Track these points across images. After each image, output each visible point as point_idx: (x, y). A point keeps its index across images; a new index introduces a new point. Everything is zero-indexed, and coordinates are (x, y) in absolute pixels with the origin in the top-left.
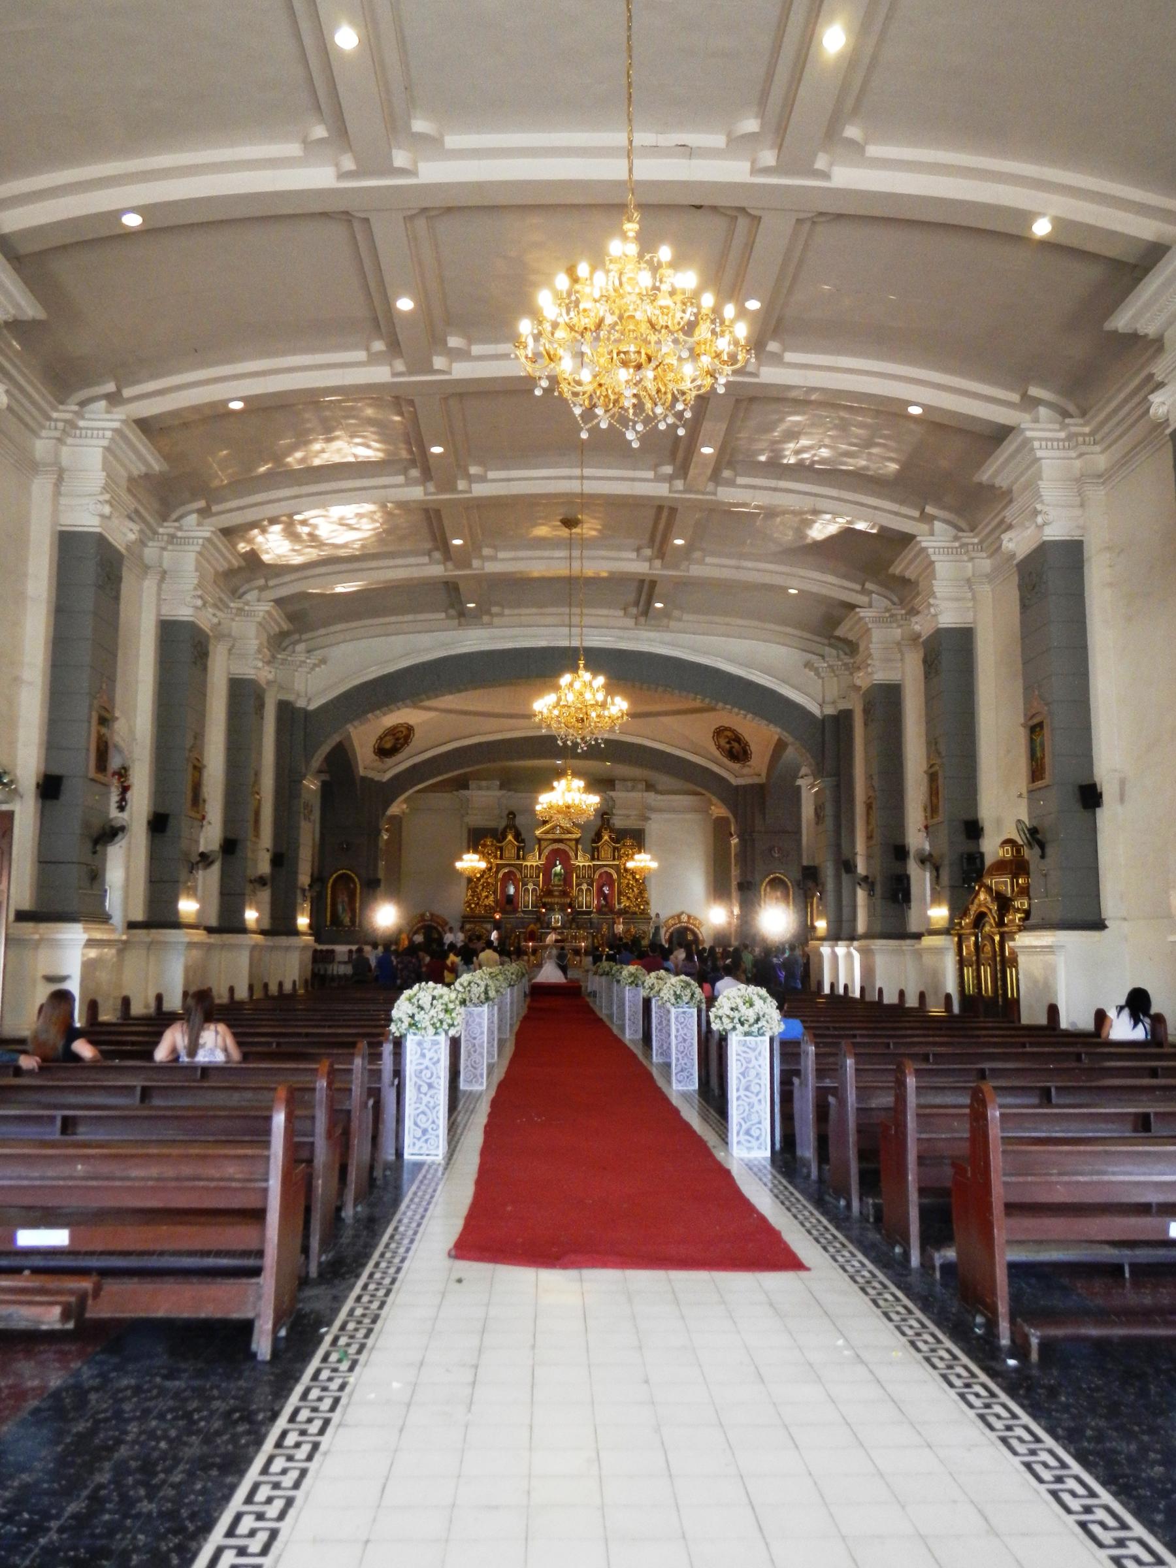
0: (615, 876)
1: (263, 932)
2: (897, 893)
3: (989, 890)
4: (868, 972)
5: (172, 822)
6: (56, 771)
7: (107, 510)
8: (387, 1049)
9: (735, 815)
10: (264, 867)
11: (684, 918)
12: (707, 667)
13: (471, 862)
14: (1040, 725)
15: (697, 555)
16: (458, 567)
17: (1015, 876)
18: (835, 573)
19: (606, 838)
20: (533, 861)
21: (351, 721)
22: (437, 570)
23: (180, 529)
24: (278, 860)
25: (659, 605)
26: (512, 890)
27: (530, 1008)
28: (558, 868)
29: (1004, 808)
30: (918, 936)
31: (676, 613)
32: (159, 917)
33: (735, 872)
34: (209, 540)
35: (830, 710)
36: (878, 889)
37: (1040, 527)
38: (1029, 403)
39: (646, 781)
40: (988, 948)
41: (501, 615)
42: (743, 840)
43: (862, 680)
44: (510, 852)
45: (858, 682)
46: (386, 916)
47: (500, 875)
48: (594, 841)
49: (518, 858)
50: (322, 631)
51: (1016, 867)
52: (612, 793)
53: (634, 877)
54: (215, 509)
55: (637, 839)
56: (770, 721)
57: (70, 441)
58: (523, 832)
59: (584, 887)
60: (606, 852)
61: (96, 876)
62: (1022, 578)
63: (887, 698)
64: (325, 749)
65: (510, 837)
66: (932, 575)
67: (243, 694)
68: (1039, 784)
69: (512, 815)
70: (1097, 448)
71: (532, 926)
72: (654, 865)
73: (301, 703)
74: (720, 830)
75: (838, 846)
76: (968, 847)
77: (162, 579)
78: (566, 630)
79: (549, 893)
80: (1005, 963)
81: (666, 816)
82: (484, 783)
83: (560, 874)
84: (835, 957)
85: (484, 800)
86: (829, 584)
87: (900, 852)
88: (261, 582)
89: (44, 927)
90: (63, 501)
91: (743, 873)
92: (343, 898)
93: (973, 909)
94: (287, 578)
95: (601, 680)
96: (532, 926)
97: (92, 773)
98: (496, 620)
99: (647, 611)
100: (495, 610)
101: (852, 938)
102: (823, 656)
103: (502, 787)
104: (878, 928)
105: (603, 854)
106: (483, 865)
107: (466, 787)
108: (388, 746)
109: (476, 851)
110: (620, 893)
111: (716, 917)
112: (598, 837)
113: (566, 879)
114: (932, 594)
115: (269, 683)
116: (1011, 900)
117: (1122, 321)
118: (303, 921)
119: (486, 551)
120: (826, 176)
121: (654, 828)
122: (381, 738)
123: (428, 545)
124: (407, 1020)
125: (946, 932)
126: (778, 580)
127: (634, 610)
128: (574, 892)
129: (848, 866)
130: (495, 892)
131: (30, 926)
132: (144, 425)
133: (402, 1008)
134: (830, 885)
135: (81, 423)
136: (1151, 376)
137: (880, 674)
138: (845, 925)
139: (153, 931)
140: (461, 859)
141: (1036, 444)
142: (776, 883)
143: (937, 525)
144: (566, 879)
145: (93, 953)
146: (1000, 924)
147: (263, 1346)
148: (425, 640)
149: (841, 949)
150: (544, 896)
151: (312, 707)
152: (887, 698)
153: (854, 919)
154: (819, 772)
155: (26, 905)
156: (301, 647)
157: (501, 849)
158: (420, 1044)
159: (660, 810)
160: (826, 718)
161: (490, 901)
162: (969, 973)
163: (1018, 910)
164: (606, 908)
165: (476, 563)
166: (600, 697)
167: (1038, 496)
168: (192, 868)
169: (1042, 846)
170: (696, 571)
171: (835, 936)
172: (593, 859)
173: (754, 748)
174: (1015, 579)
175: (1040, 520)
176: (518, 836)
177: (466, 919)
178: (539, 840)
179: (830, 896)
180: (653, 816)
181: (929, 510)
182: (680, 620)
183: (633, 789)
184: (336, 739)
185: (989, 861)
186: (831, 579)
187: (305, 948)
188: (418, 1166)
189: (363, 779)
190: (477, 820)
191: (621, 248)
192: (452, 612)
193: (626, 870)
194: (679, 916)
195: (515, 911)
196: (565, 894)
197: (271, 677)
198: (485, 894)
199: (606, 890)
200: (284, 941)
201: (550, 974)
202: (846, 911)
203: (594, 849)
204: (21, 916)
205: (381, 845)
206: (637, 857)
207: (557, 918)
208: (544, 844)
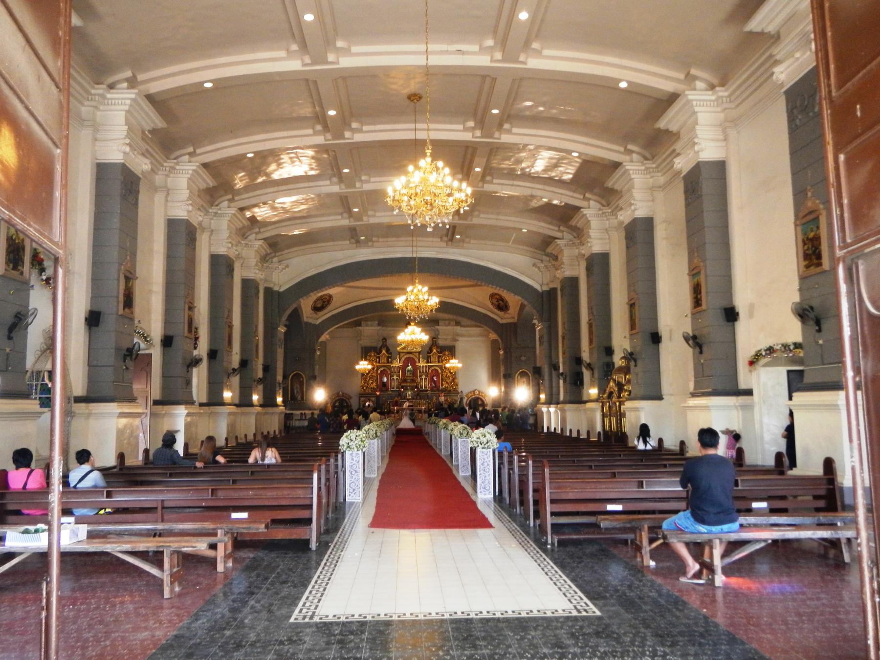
1: (261, 406)
2: (577, 382)
3: (614, 380)
4: (564, 420)
5: (219, 355)
6: (170, 333)
7: (190, 208)
8: (340, 456)
9: (502, 340)
10: (260, 374)
11: (477, 392)
12: (483, 267)
13: (363, 366)
14: (634, 304)
15: (476, 213)
16: (355, 221)
17: (626, 374)
18: (544, 221)
20: (396, 364)
21: (302, 297)
22: (345, 222)
23: (220, 209)
24: (266, 369)
25: (458, 237)
26: (385, 380)
27: (396, 441)
28: (410, 367)
29: (621, 341)
30: (585, 402)
31: (467, 240)
32: (214, 400)
33: (502, 369)
34: (234, 214)
35: (545, 288)
36: (568, 379)
37: (634, 211)
38: (630, 152)
40: (614, 409)
41: (378, 241)
42: (505, 352)
43: (560, 274)
44: (384, 360)
45: (558, 276)
46: (320, 395)
48: (428, 353)
50: (286, 251)
51: (626, 370)
54: (236, 198)
55: (451, 351)
56: (515, 294)
57: (172, 175)
58: (390, 348)
59: (424, 377)
60: (434, 358)
61: (189, 383)
62: (626, 234)
63: (573, 283)
64: (288, 312)
65: (384, 351)
66: (589, 227)
67: (248, 285)
68: (634, 332)
69: (385, 339)
70: (660, 174)
72: (460, 365)
73: (276, 288)
74: (494, 347)
75: (550, 357)
76: (607, 359)
77: (211, 235)
78: (410, 249)
80: (621, 416)
81: (466, 339)
82: (369, 323)
84: (549, 412)
85: (370, 332)
86: (544, 227)
87: (578, 361)
88: (257, 230)
89: (166, 407)
90: (169, 204)
91: (506, 369)
92: (297, 386)
93: (608, 390)
94: (270, 228)
95: (426, 289)
97: (186, 334)
98: (375, 244)
99: (452, 239)
100: (374, 239)
101: (558, 403)
102: (542, 261)
103: (379, 325)
104: (568, 398)
106: (370, 367)
108: (319, 305)
109: (366, 360)
110: (442, 380)
111: (493, 393)
112: (431, 350)
113: (414, 373)
114: (589, 237)
115: (261, 280)
116: (624, 385)
117: (662, 124)
118: (279, 400)
119: (370, 213)
120: (524, 63)
121: (460, 345)
122: (315, 302)
123: (341, 210)
124: (346, 445)
125: (596, 401)
126: (518, 226)
127: (445, 239)
128: (418, 380)
129: (555, 367)
130: (376, 381)
131: (160, 407)
132: (205, 166)
133: (343, 441)
134: (546, 377)
135: (177, 167)
136: (674, 150)
137: (568, 273)
138: (554, 397)
139: (211, 407)
140: (358, 364)
141: (631, 172)
142: (523, 374)
143: (592, 203)
144: (414, 373)
145: (189, 419)
146: (619, 397)
147: (313, 546)
148: (339, 254)
149: (552, 409)
151: (281, 290)
152: (573, 283)
153: (559, 394)
154: (541, 320)
155: (158, 398)
156: (275, 260)
157: (379, 358)
158: (351, 454)
159: (463, 336)
160: (543, 292)
162: (606, 420)
163: (626, 391)
164: (436, 388)
165: (365, 218)
166: (426, 297)
167: (632, 196)
168: (229, 376)
169: (635, 361)
170: (475, 221)
171: (549, 403)
172: (428, 362)
173: (511, 304)
174: (624, 234)
175: (633, 207)
176: (388, 351)
177: (361, 395)
178: (399, 353)
179: (547, 383)
180: (460, 339)
181: (587, 195)
182: (469, 242)
184: (295, 306)
185: (616, 366)
186: (543, 224)
187: (281, 413)
188: (352, 504)
189: (306, 323)
190: (366, 342)
191: (425, 162)
192: (353, 241)
194: (474, 392)
195: (387, 390)
196: (413, 381)
197: (262, 277)
199: (435, 378)
200: (270, 410)
201: (406, 423)
202: (554, 390)
204: (156, 403)
205: (316, 357)
206: (451, 361)
207: (409, 394)
208: (402, 355)
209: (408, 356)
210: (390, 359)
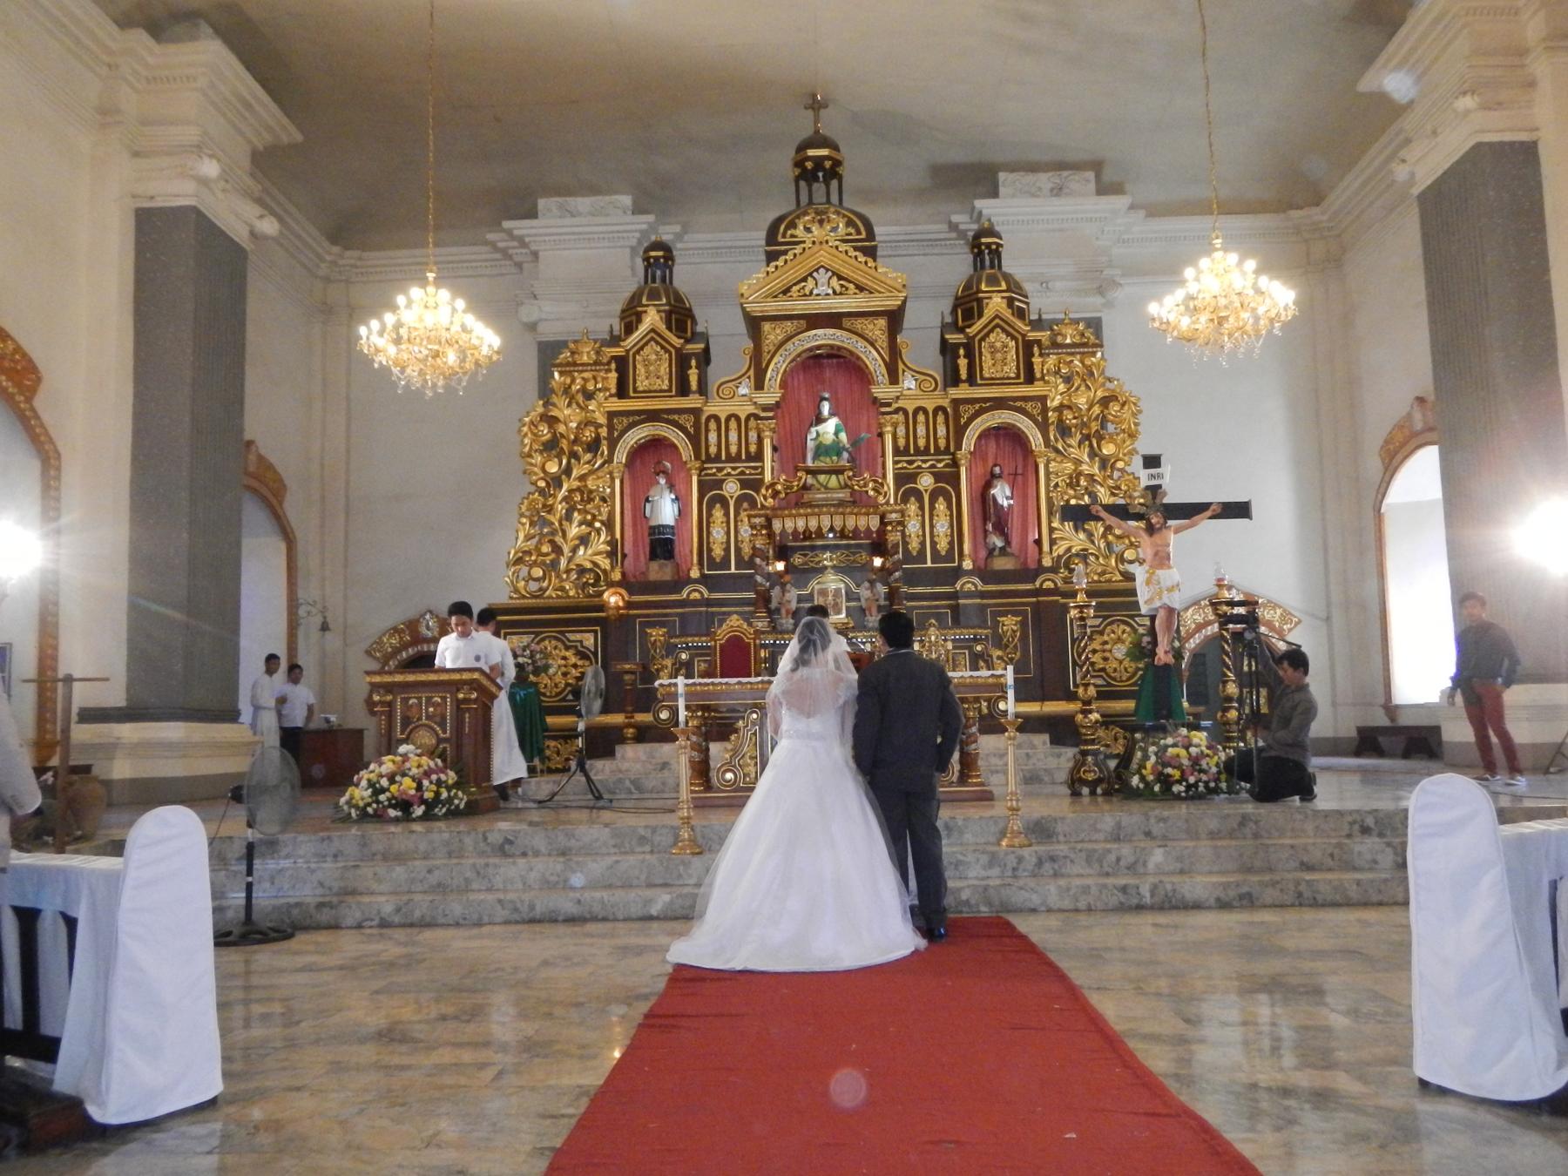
0: (1035, 438)
19: (996, 304)
20: (735, 397)
26: (665, 511)
39: (1097, 166)
47: (621, 456)
49: (684, 390)
52: (985, 206)
53: (1093, 454)
59: (926, 482)
60: (998, 357)
65: (652, 318)
69: (659, 259)
71: (734, 621)
79: (797, 500)
82: (583, 203)
83: (836, 449)
96: (734, 621)
103: (638, 209)
105: (988, 368)
107: (532, 214)
113: (862, 455)
130: (609, 525)
144: (862, 455)
150: (776, 512)
161: (595, 553)
172: (952, 379)
178: (754, 324)
183: (1057, 191)
193: (1064, 431)
198: (574, 531)
199: (1001, 493)
203: (947, 349)
209: (823, 337)
210: (691, 363)
